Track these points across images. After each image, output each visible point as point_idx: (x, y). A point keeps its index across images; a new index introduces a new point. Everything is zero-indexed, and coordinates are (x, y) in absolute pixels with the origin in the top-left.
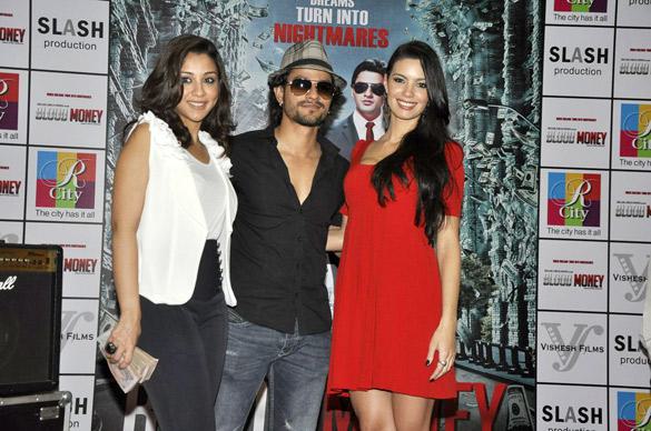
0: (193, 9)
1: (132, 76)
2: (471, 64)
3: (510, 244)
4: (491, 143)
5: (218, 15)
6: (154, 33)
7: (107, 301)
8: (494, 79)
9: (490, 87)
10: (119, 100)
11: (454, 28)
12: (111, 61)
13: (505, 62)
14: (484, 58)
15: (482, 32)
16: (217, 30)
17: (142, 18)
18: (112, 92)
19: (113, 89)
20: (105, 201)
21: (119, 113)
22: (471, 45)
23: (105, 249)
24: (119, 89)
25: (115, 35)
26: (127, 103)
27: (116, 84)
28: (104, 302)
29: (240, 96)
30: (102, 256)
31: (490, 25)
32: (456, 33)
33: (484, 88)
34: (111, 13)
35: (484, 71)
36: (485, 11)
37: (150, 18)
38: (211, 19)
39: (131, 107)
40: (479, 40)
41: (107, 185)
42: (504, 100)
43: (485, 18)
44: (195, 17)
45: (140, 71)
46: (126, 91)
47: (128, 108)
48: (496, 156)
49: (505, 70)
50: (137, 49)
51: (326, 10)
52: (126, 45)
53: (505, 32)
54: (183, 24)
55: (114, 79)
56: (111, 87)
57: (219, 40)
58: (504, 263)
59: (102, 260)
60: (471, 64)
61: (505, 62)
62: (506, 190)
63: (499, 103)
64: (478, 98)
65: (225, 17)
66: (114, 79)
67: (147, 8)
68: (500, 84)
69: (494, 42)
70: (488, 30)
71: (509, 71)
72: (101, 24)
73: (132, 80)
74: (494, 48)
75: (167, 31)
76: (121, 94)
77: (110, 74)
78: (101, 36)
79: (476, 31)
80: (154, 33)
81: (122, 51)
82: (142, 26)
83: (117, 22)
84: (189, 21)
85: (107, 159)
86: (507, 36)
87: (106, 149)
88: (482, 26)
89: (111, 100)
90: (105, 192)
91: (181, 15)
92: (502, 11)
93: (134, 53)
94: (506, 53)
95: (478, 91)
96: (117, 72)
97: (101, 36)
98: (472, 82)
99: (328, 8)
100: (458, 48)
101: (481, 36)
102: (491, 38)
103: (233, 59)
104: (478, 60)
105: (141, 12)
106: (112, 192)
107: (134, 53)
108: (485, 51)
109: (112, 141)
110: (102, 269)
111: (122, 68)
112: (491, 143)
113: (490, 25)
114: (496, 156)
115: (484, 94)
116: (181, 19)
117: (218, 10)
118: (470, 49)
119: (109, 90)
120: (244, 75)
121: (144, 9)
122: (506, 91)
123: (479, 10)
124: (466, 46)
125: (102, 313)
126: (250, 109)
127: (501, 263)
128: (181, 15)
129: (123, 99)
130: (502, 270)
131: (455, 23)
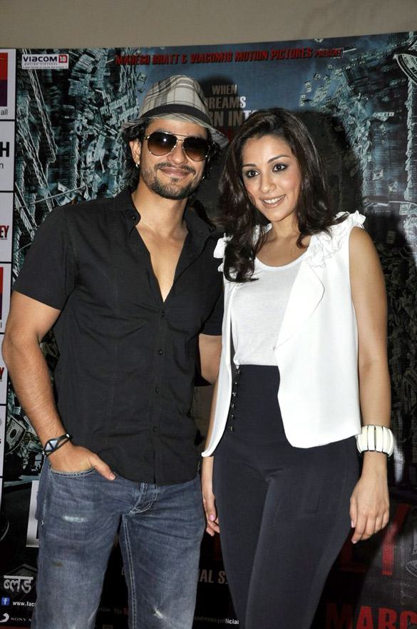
0: (90, 122)
2: (370, 158)
3: (414, 351)
4: (392, 242)
5: (113, 127)
6: (54, 148)
7: (13, 408)
8: (396, 172)
9: (391, 182)
10: (23, 215)
11: (351, 120)
12: (16, 179)
13: (409, 153)
14: (385, 150)
15: (381, 122)
16: (111, 140)
17: (44, 135)
18: (17, 207)
19: (18, 205)
21: (23, 228)
22: (371, 137)
24: (23, 204)
25: (20, 154)
26: (30, 218)
27: (21, 200)
28: (10, 408)
31: (392, 114)
32: (354, 127)
33: (385, 183)
34: (16, 132)
35: (385, 165)
36: (386, 99)
37: (51, 135)
38: (107, 131)
39: (34, 221)
40: (380, 132)
42: (407, 194)
43: (385, 107)
44: (91, 130)
45: (42, 186)
46: (30, 206)
47: (31, 222)
48: (398, 256)
49: (408, 162)
50: (39, 165)
51: (217, 113)
52: (30, 162)
53: (408, 120)
54: (80, 138)
55: (19, 195)
57: (114, 151)
58: (407, 372)
60: (370, 158)
61: (409, 153)
62: (409, 293)
63: (401, 198)
64: (378, 194)
65: (119, 128)
66: (19, 195)
67: (48, 125)
68: (402, 178)
69: (396, 133)
70: (390, 120)
71: (413, 163)
72: (8, 144)
73: (34, 196)
74: (394, 139)
75: (66, 146)
76: (25, 209)
77: (15, 191)
78: (8, 155)
79: (376, 122)
80: (54, 148)
81: (26, 168)
82: (43, 144)
83: (22, 141)
84: (85, 135)
85: (12, 272)
86: (410, 124)
87: (13, 263)
88: (383, 116)
89: (16, 215)
91: (78, 130)
92: (405, 98)
93: (36, 169)
94: (409, 144)
95: (378, 186)
96: (21, 189)
97: (8, 155)
98: (371, 177)
99: (219, 110)
100: (356, 142)
101: (382, 127)
102: (392, 128)
104: (378, 154)
105: (42, 130)
107: (36, 169)
108: (386, 144)
109: (17, 254)
111: (26, 184)
112: (392, 242)
113: (392, 114)
114: (398, 256)
115: (384, 190)
116: (79, 133)
117: (113, 121)
118: (368, 142)
119: (14, 205)
121: (45, 126)
122: (410, 184)
123: (380, 99)
124: (365, 139)
125: (9, 420)
127: (403, 372)
128: (78, 130)
129: (27, 213)
130: (405, 380)
131: (353, 115)
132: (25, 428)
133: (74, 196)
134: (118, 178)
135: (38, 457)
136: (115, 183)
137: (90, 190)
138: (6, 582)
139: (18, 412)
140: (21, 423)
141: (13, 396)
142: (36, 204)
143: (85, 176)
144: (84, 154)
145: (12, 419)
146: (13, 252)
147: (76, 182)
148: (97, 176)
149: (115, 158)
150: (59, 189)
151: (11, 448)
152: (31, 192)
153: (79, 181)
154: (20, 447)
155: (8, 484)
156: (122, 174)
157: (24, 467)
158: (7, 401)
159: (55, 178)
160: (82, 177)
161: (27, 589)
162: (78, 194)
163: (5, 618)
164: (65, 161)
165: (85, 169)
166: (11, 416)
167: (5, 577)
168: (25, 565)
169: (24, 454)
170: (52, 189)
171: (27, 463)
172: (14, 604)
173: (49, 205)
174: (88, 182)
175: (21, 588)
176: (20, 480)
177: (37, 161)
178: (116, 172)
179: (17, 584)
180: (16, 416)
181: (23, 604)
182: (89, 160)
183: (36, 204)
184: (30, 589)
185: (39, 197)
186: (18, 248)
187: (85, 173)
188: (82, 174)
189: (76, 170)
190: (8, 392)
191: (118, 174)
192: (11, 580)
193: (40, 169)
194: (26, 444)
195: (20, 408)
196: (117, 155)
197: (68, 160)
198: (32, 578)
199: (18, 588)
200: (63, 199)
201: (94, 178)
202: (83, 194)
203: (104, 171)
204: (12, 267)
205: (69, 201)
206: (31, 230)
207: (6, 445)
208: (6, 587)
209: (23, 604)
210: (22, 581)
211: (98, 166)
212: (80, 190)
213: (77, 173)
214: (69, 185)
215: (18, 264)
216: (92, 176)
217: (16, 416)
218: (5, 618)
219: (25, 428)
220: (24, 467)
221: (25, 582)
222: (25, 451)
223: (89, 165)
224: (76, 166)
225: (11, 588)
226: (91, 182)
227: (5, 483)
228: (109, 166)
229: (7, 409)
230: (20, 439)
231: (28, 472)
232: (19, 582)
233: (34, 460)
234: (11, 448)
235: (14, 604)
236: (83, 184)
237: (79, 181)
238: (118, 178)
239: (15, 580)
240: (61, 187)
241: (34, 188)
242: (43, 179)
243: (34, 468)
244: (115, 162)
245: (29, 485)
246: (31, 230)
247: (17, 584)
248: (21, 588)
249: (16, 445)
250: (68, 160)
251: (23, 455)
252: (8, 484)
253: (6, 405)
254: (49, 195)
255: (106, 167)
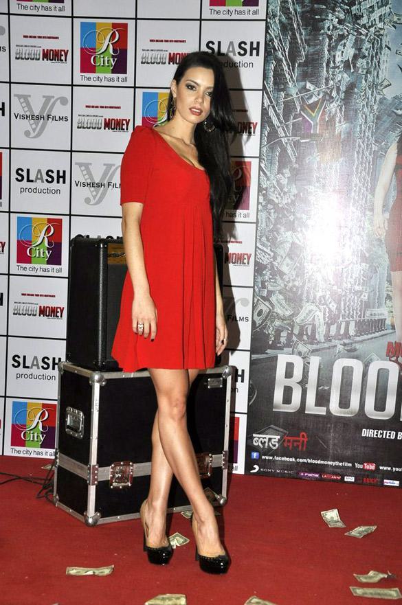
1: (283, 90)
10: (271, 113)
12: (265, 77)
18: (266, 105)
19: (267, 102)
20: (258, 203)
21: (271, 125)
23: (258, 245)
24: (271, 102)
26: (278, 115)
28: (257, 290)
29: (381, 102)
30: (256, 251)
39: (282, 118)
41: (260, 189)
45: (290, 84)
47: (279, 119)
50: (288, 65)
55: (267, 93)
56: (265, 101)
59: (256, 255)
66: (267, 93)
73: (283, 94)
76: (273, 107)
77: (264, 89)
81: (275, 67)
85: (260, 167)
90: (258, 195)
93: (286, 68)
103: (375, 69)
106: (264, 195)
107: (286, 68)
109: (264, 149)
110: (255, 261)
111: (275, 83)
119: (263, 103)
120: (386, 83)
126: (389, 115)
129: (275, 111)
132: (271, 308)
133: (321, 95)
134: (366, 77)
135: (284, 334)
136: (364, 82)
137: (338, 89)
138: (255, 439)
139: (265, 294)
140: (267, 303)
141: (259, 279)
142: (284, 102)
143: (333, 75)
144: (333, 54)
145: (258, 300)
146: (260, 148)
147: (324, 81)
148: (345, 75)
149: (364, 57)
150: (308, 87)
151: (257, 325)
152: (279, 90)
153: (327, 80)
154: (266, 325)
155: (255, 357)
156: (370, 73)
157: (270, 342)
158: (254, 284)
159: (305, 76)
160: (331, 76)
161: (275, 446)
162: (326, 93)
163: (255, 469)
164: (314, 60)
165: (333, 68)
166: (258, 297)
167: (254, 435)
168: (272, 426)
169: (271, 331)
170: (300, 87)
171: (273, 339)
172: (263, 457)
173: (297, 103)
174: (337, 81)
175: (269, 445)
176: (267, 353)
177: (286, 60)
178: (365, 71)
179: (265, 442)
180: (263, 298)
181: (271, 458)
182: (338, 59)
183: (284, 102)
184: (277, 446)
185: (287, 95)
186: (266, 143)
187: (333, 72)
188: (331, 73)
189: (325, 69)
190: (255, 276)
191: (367, 72)
192: (259, 438)
193: (289, 69)
194: (272, 322)
195: (266, 290)
196: (367, 54)
197: (318, 59)
198: (279, 437)
199: (267, 444)
200: (312, 96)
201: (342, 77)
202: (331, 92)
203: (352, 70)
204: (260, 162)
205: (316, 99)
206: (278, 127)
207: (254, 323)
208: (255, 444)
209: (271, 458)
210: (270, 439)
211: (347, 65)
212: (328, 88)
213: (325, 72)
214: (317, 84)
215: (265, 158)
216: (340, 75)
217: (263, 298)
218: (255, 469)
219: (271, 308)
220: (270, 342)
221: (273, 440)
222: (271, 328)
223: (337, 65)
224: (324, 65)
225: (260, 444)
226: (339, 81)
227: (253, 356)
228: (358, 65)
229: (254, 290)
230: (266, 318)
231: (274, 347)
232: (267, 440)
233: (280, 336)
234: (257, 325)
235: (263, 457)
236: (331, 83)
237: (327, 80)
238: (366, 77)
239: (264, 438)
240: (309, 86)
241: (283, 87)
242: (292, 77)
243: (280, 343)
244: (364, 61)
245: (275, 359)
246: (278, 127)
247: (265, 442)
248: (269, 445)
249: (263, 322)
250: (318, 59)
251: (270, 332)
252: (255, 357)
253: (253, 287)
254: (297, 94)
255: (354, 66)
